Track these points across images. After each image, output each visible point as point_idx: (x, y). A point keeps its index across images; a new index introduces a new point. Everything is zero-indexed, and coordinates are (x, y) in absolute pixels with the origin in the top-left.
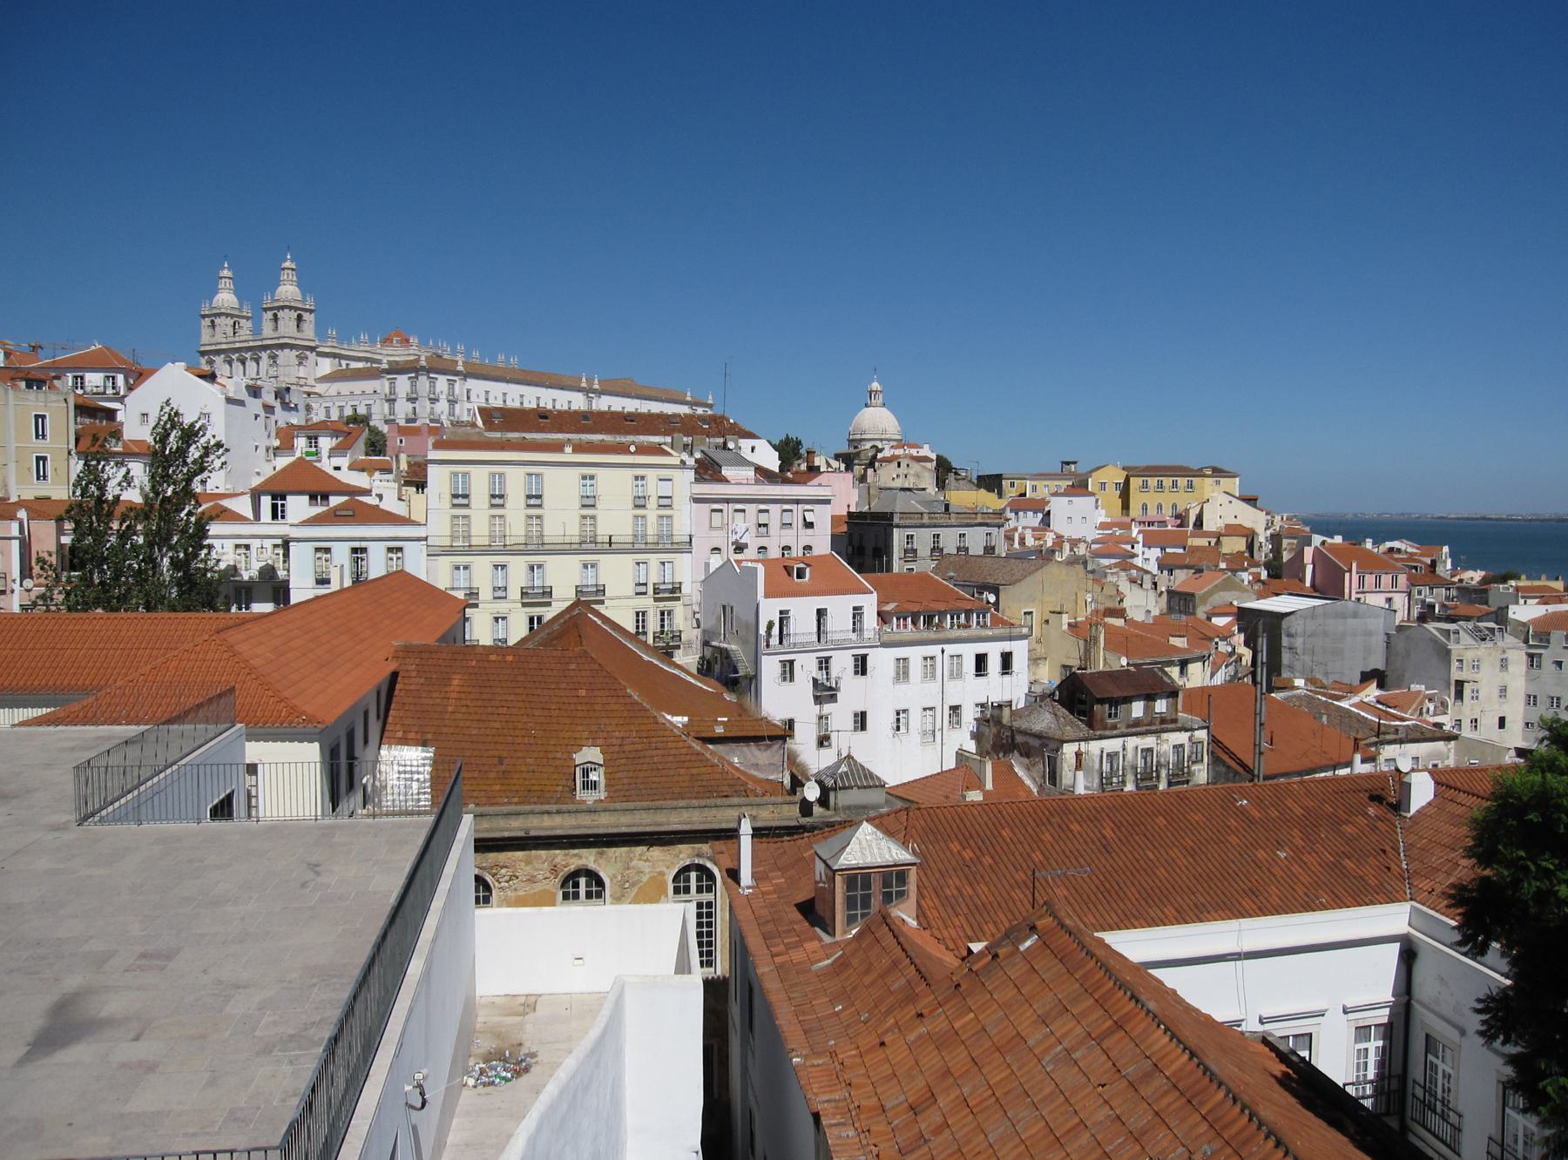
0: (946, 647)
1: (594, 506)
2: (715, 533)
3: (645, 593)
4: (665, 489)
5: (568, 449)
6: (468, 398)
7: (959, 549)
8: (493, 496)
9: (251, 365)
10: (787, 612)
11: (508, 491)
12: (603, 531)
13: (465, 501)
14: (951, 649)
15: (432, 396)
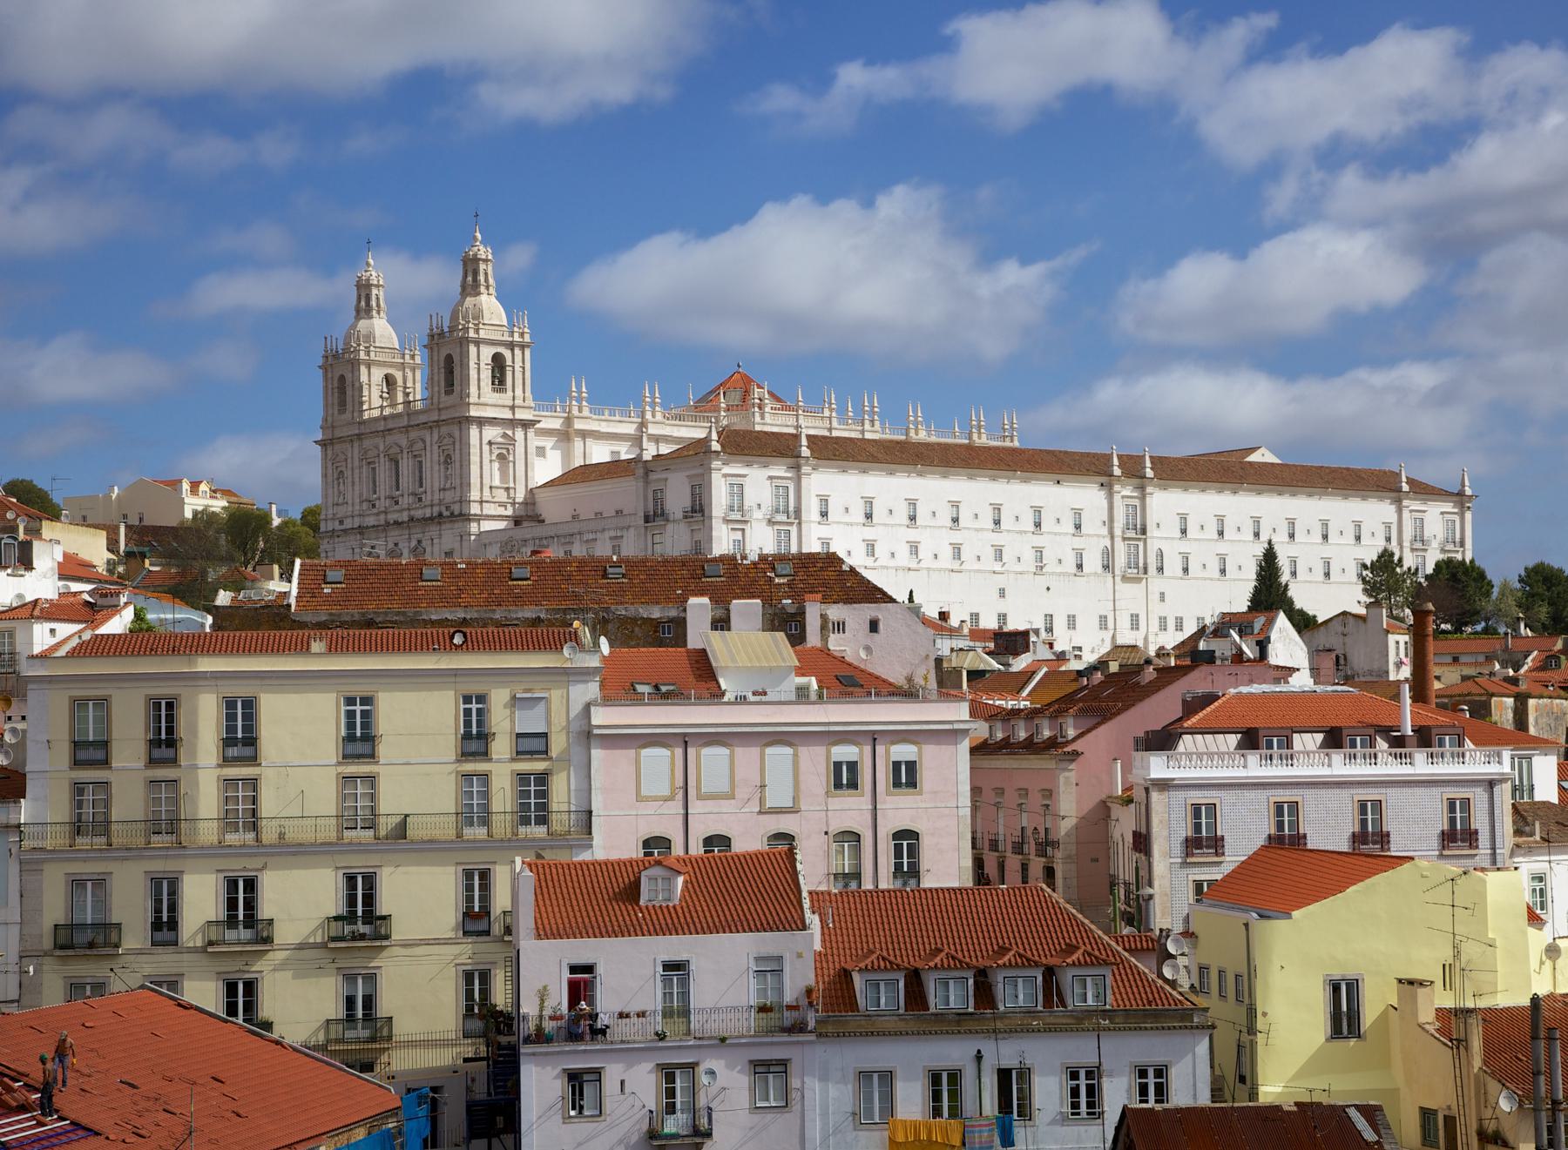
0: (988, 1047)
1: (372, 756)
2: (650, 808)
3: (487, 933)
4: (531, 722)
5: (316, 647)
6: (824, 514)
7: (1359, 838)
8: (155, 743)
9: (406, 466)
10: (589, 969)
11: (182, 731)
12: (391, 803)
13: (100, 755)
14: (1007, 1053)
15: (736, 516)
